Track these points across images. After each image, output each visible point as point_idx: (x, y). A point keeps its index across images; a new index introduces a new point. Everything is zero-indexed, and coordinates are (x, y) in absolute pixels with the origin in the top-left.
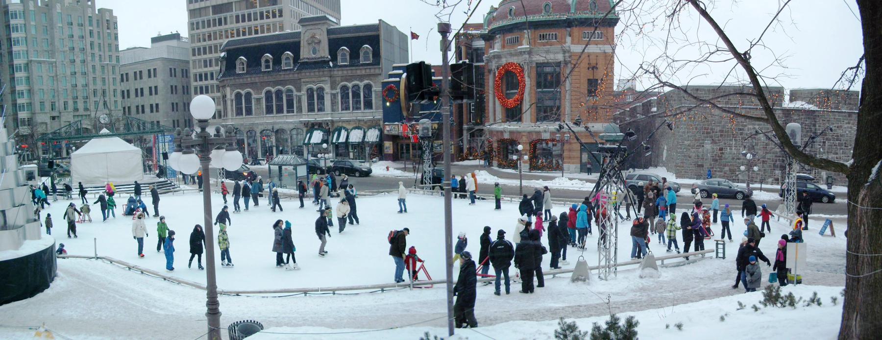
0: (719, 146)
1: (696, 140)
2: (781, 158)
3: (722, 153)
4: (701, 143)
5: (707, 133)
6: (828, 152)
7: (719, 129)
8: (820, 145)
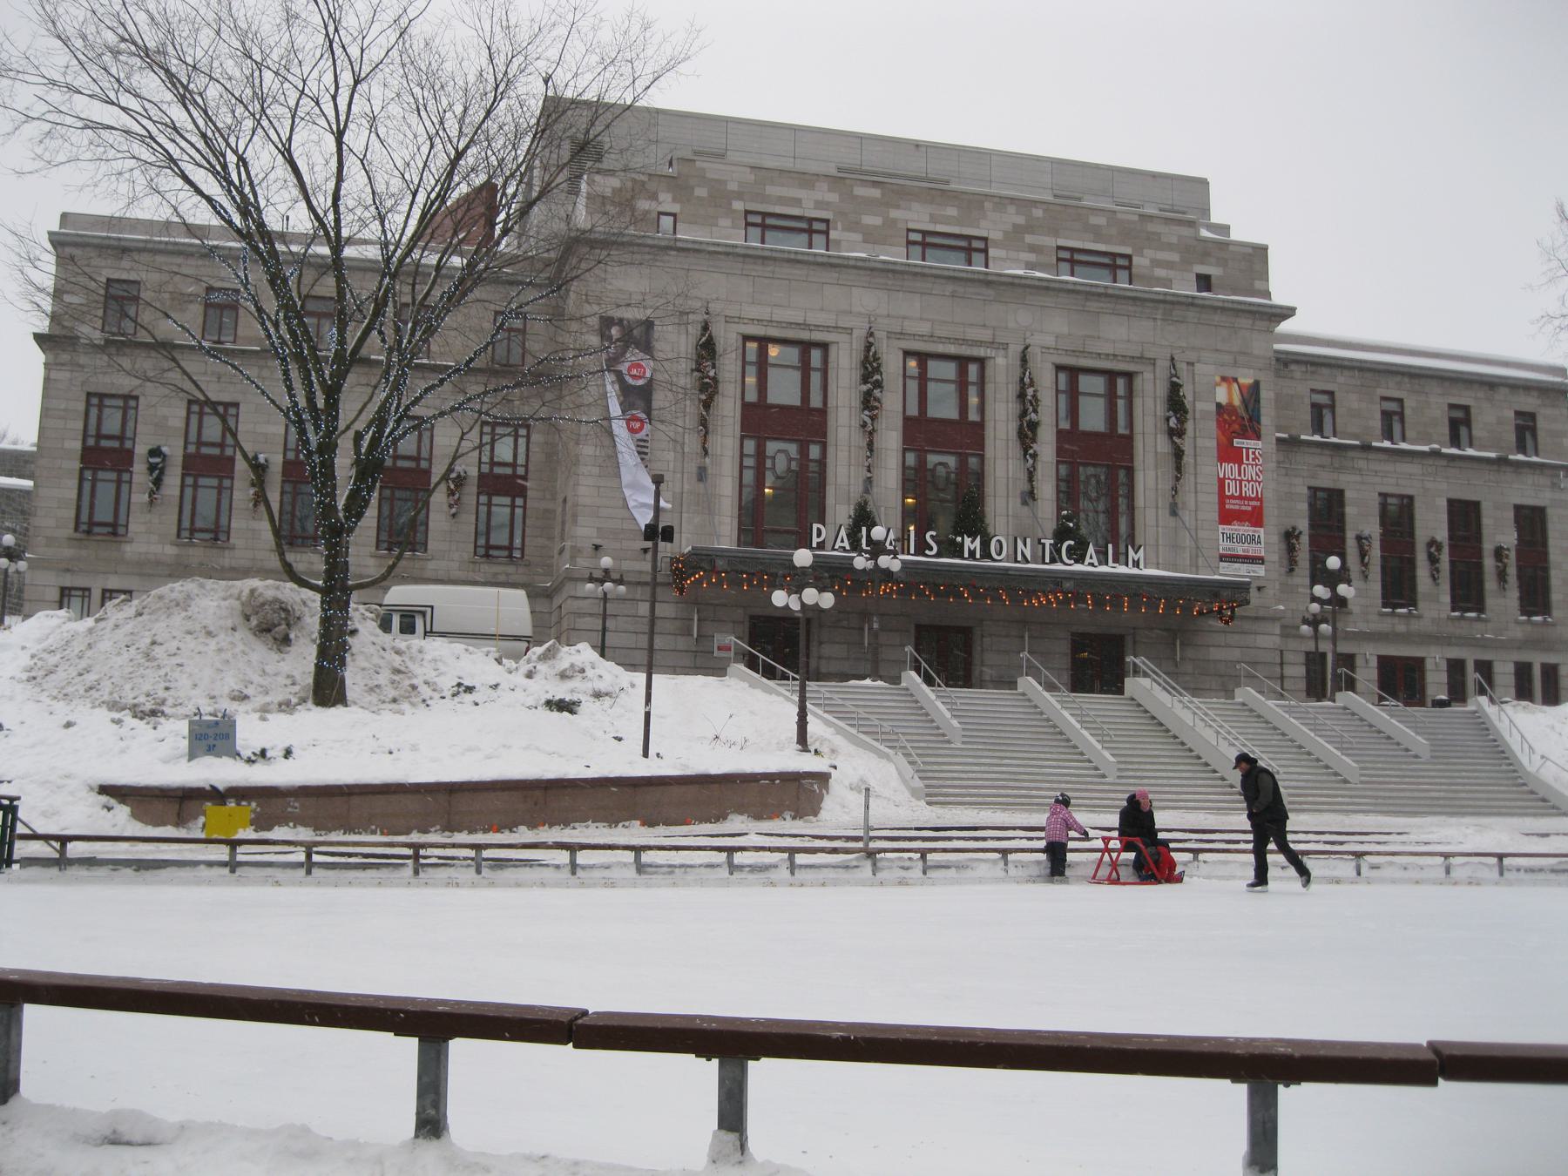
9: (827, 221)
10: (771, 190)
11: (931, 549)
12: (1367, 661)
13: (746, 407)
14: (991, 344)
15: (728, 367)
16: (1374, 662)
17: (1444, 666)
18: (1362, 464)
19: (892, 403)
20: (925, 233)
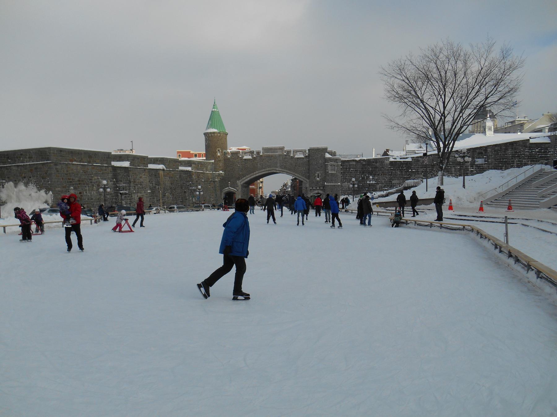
0: (79, 191)
1: (63, 187)
2: (115, 197)
3: (81, 196)
4: (67, 189)
5: (71, 182)
6: (137, 192)
7: (77, 179)
8: (133, 188)
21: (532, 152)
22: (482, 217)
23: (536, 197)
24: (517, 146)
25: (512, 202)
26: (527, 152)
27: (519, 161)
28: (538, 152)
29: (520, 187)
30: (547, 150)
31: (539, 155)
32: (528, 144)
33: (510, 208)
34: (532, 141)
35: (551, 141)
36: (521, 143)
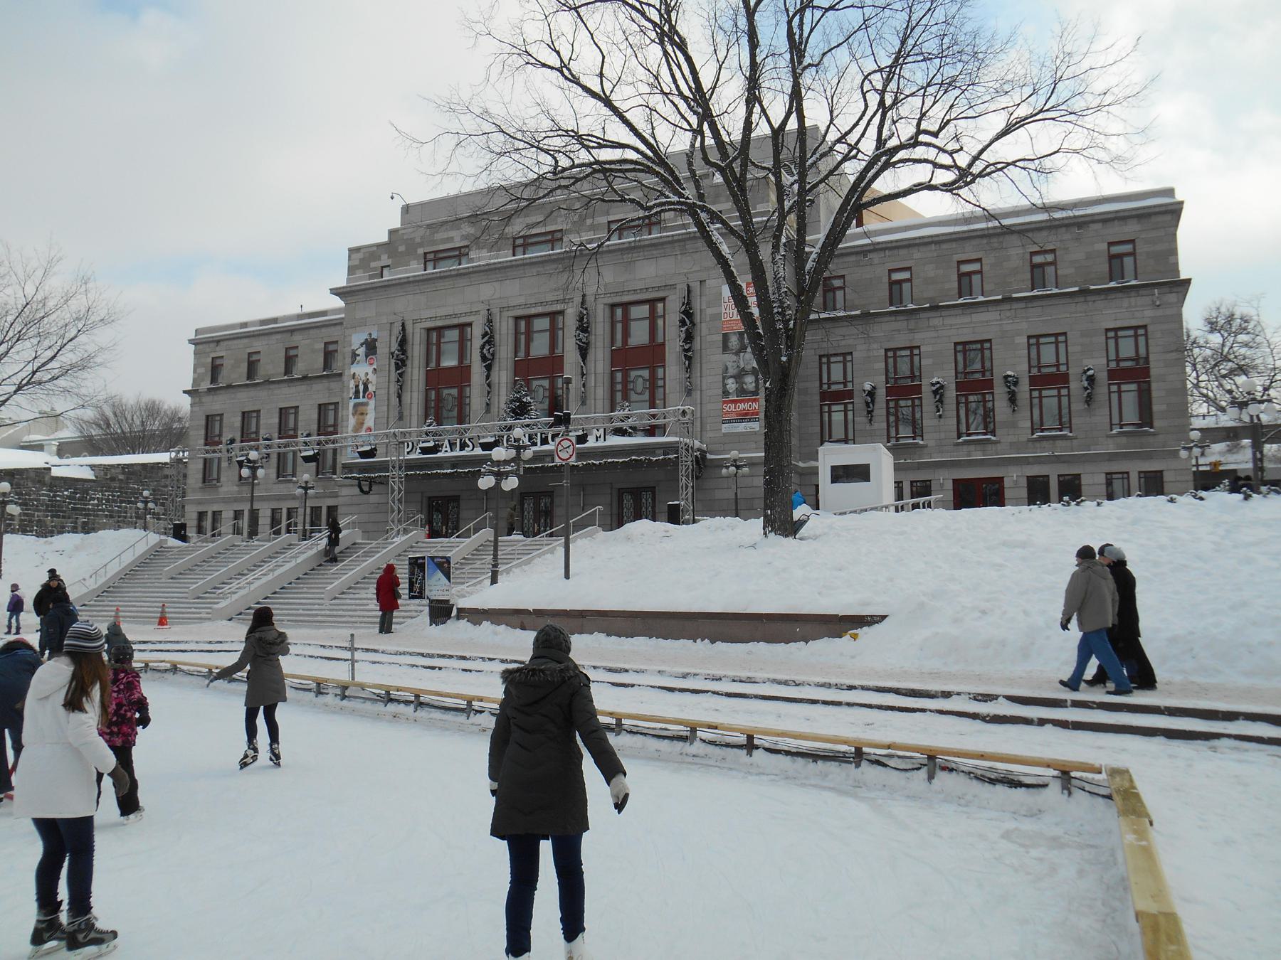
9: (467, 246)
10: (439, 236)
11: (468, 446)
12: (942, 485)
13: (614, 354)
14: (564, 301)
15: (417, 350)
16: (949, 485)
17: (1024, 482)
18: (935, 322)
19: (505, 351)
20: (524, 237)
21: (55, 496)
22: (144, 642)
23: (186, 598)
24: (23, 479)
25: (167, 610)
26: (44, 495)
27: (25, 515)
28: (68, 497)
29: (127, 576)
30: (87, 495)
31: (70, 503)
32: (47, 478)
33: (162, 621)
34: (56, 472)
35: (96, 477)
36: (32, 474)
